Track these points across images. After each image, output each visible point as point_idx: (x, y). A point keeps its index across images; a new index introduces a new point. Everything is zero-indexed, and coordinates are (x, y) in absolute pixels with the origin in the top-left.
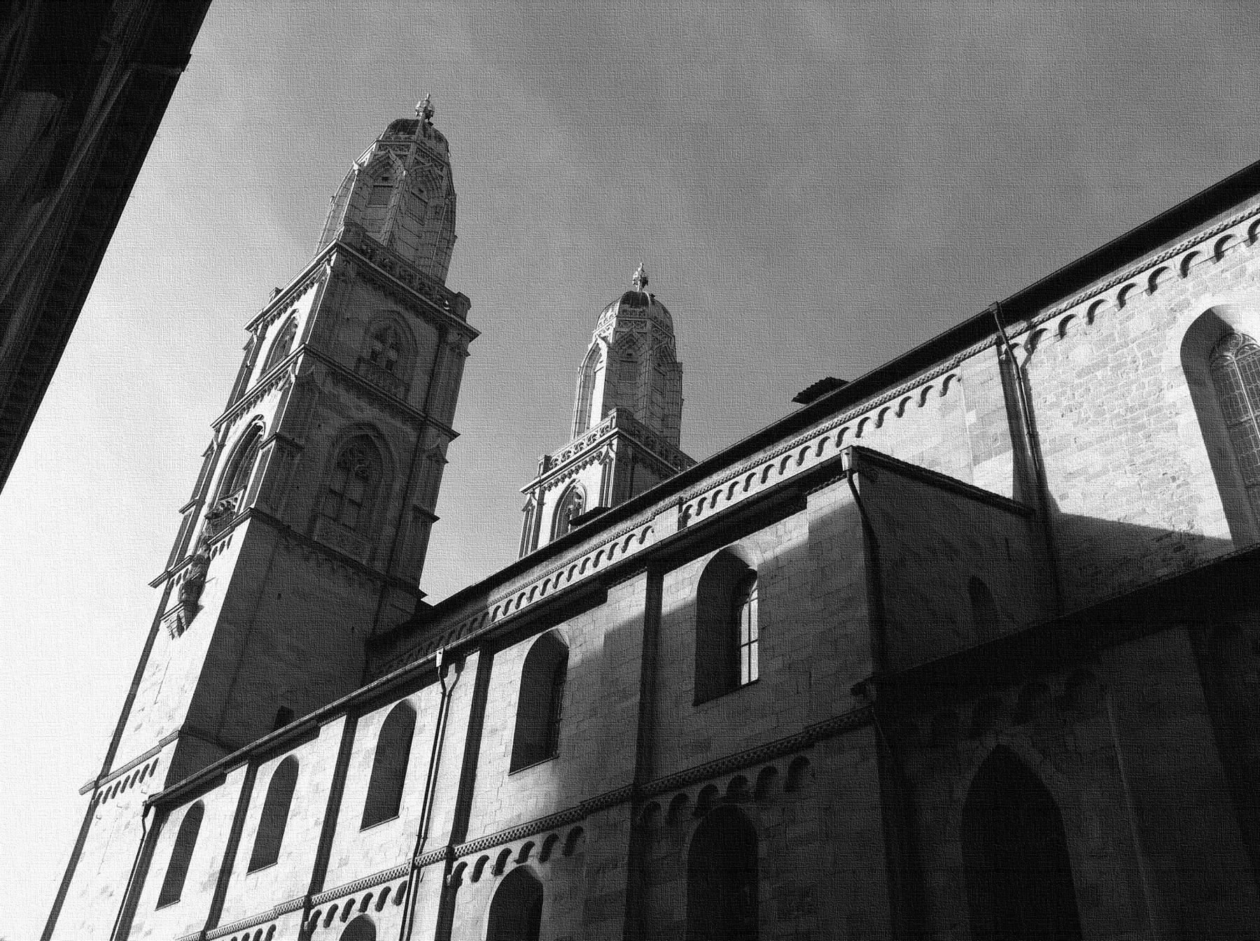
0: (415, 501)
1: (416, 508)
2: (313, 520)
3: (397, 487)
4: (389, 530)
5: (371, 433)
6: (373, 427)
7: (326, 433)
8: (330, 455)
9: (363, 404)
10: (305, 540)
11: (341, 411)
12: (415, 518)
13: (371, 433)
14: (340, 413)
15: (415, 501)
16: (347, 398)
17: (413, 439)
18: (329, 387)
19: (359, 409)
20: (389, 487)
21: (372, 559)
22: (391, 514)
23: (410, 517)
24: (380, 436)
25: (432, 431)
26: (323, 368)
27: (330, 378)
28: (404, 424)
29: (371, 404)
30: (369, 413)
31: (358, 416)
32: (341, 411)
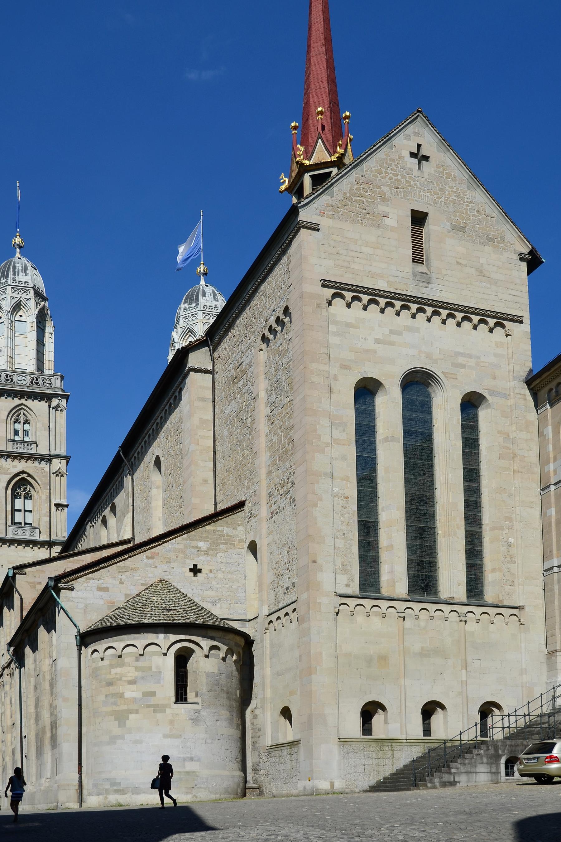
24: (30, 476)
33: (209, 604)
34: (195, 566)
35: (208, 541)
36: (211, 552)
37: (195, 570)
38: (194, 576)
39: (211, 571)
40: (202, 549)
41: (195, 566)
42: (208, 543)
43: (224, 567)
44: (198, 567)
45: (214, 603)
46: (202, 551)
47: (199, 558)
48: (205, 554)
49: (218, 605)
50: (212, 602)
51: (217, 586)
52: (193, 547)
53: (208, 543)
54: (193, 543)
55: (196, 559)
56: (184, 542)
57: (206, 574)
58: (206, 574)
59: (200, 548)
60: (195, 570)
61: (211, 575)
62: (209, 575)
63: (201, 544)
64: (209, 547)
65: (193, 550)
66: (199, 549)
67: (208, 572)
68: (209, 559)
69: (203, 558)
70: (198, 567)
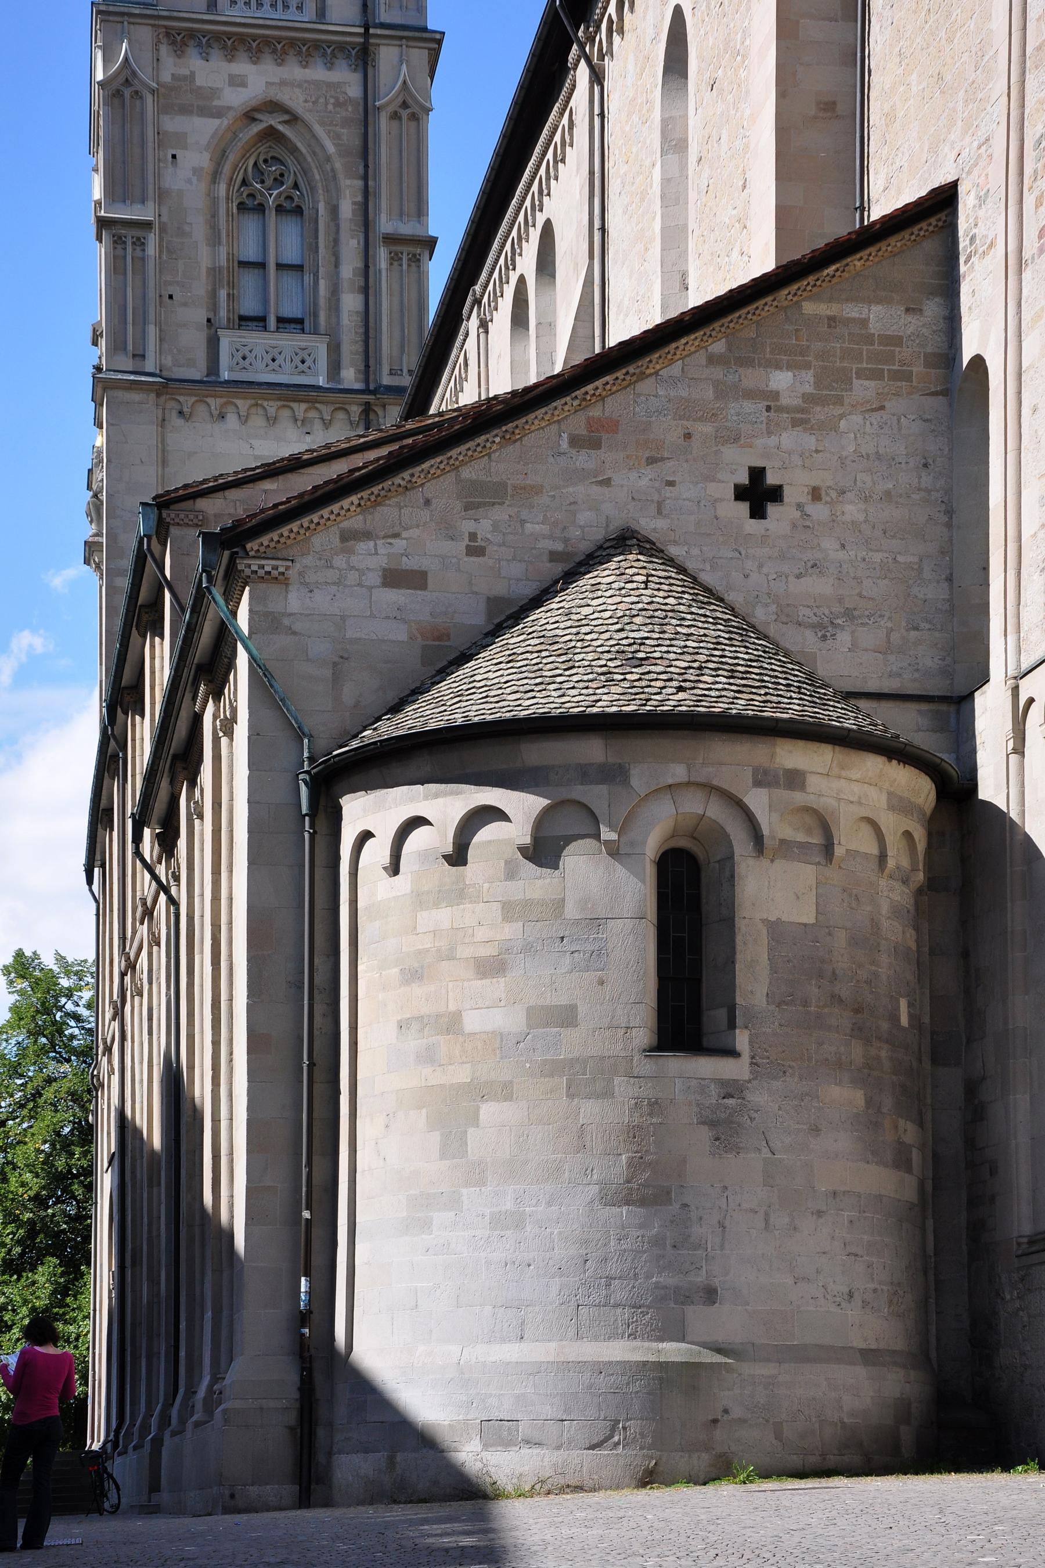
0: (386, 224)
1: (390, 240)
2: (213, 343)
3: (347, 209)
4: (351, 302)
5: (274, 121)
6: (273, 106)
7: (193, 159)
8: (214, 202)
9: (243, 67)
10: (210, 383)
11: (204, 105)
12: (395, 258)
13: (274, 121)
14: (206, 112)
15: (386, 224)
16: (209, 71)
17: (354, 91)
18: (170, 67)
19: (237, 82)
20: (334, 211)
21: (335, 368)
22: (350, 268)
23: (382, 256)
24: (293, 119)
25: (387, 55)
26: (145, 33)
27: (164, 49)
28: (330, 66)
29: (255, 60)
30: (255, 80)
31: (237, 99)
32: (204, 105)
33: (809, 633)
34: (757, 474)
35: (807, 366)
36: (819, 413)
37: (758, 494)
38: (753, 516)
39: (816, 494)
40: (785, 401)
41: (757, 474)
42: (808, 376)
43: (867, 478)
44: (771, 479)
45: (825, 629)
46: (781, 409)
47: (773, 440)
48: (796, 423)
49: (844, 638)
50: (821, 626)
51: (841, 555)
52: (750, 394)
53: (808, 376)
54: (750, 377)
55: (759, 442)
56: (718, 372)
57: (799, 506)
58: (799, 506)
59: (776, 395)
60: (758, 494)
61: (819, 511)
62: (810, 509)
63: (781, 380)
64: (808, 388)
65: (748, 406)
66: (771, 400)
67: (805, 498)
68: (810, 442)
69: (788, 439)
70: (771, 479)
